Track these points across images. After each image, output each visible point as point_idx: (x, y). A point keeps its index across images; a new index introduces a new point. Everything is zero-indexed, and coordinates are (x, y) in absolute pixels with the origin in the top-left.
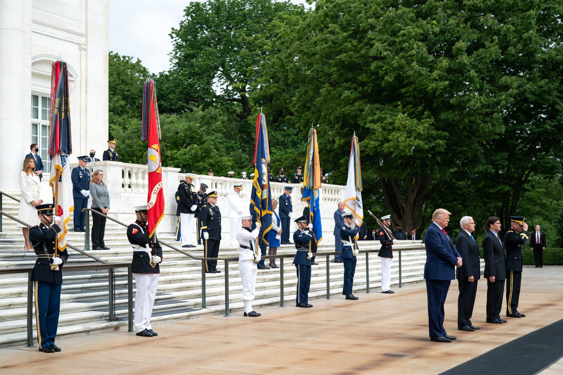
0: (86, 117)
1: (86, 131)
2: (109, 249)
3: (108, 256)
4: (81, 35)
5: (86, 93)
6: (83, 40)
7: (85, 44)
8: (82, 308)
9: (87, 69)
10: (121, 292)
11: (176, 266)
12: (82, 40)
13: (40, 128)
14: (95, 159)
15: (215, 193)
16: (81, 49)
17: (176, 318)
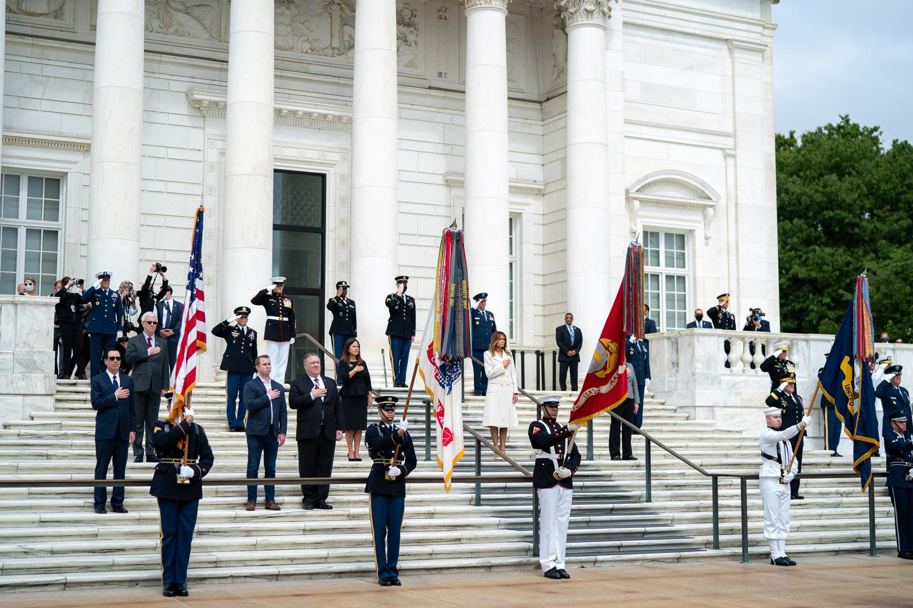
0: (737, 260)
1: (738, 280)
2: (636, 459)
3: (622, 468)
4: (726, 135)
5: (737, 221)
6: (728, 142)
7: (732, 147)
8: (507, 537)
9: (736, 186)
10: (588, 520)
11: (732, 487)
12: (728, 142)
13: (663, 280)
14: (704, 322)
15: (792, 375)
16: (726, 156)
17: (653, 560)
